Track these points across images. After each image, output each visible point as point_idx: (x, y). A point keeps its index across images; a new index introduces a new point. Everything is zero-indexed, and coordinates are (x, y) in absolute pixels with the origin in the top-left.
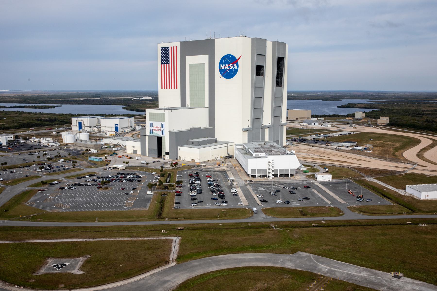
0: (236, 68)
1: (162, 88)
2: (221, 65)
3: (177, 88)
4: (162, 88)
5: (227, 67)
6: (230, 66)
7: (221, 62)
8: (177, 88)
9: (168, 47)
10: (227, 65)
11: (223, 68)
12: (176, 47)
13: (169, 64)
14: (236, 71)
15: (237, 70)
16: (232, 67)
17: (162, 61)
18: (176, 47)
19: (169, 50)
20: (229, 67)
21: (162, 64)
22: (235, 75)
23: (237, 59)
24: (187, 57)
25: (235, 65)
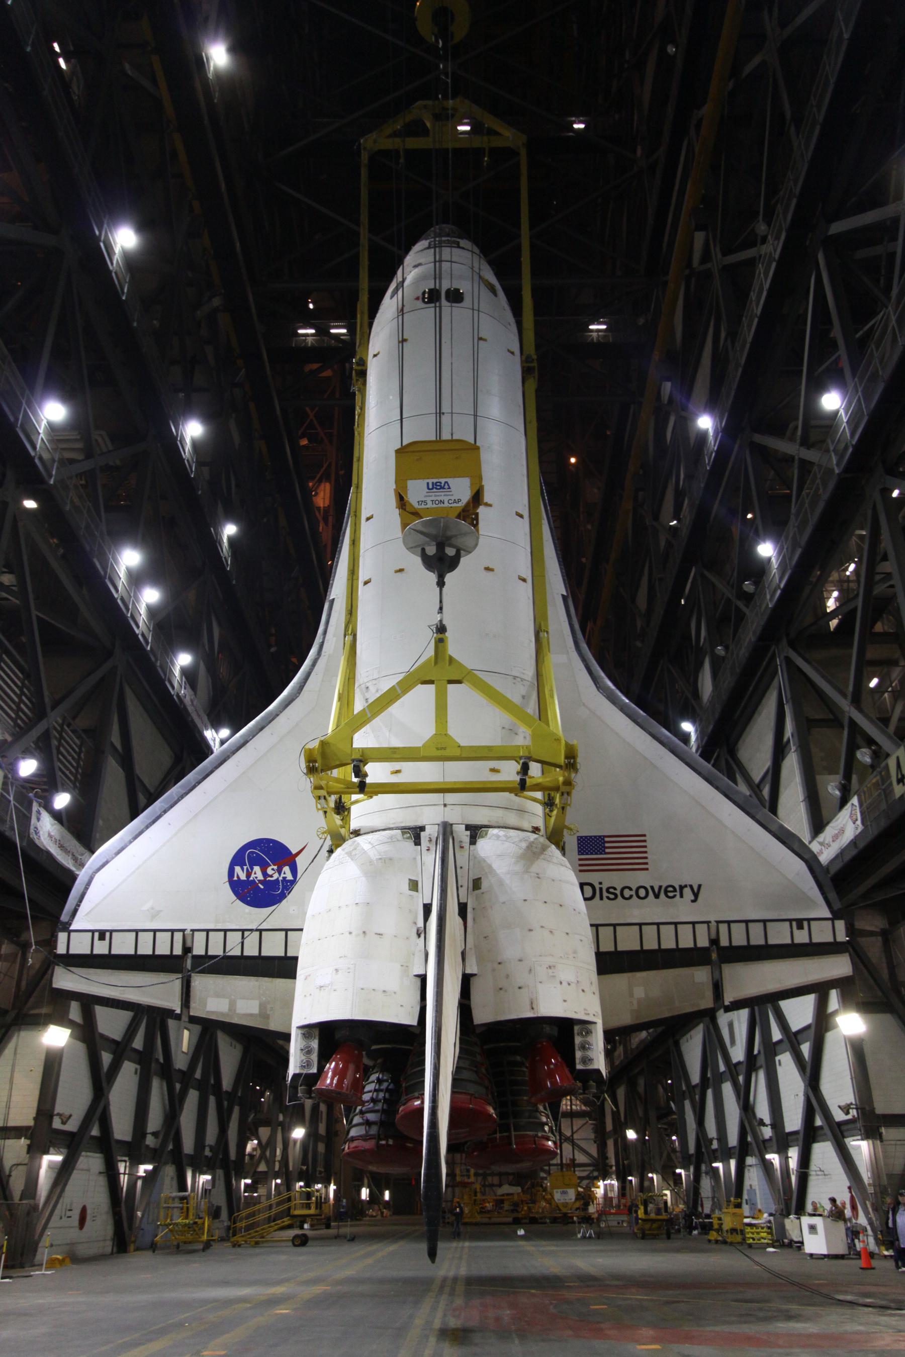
0: (289, 877)
2: (238, 869)
6: (269, 871)
7: (238, 859)
10: (257, 869)
11: (243, 877)
14: (288, 885)
15: (293, 882)
16: (276, 876)
20: (265, 874)
22: (282, 897)
23: (294, 852)
25: (286, 869)
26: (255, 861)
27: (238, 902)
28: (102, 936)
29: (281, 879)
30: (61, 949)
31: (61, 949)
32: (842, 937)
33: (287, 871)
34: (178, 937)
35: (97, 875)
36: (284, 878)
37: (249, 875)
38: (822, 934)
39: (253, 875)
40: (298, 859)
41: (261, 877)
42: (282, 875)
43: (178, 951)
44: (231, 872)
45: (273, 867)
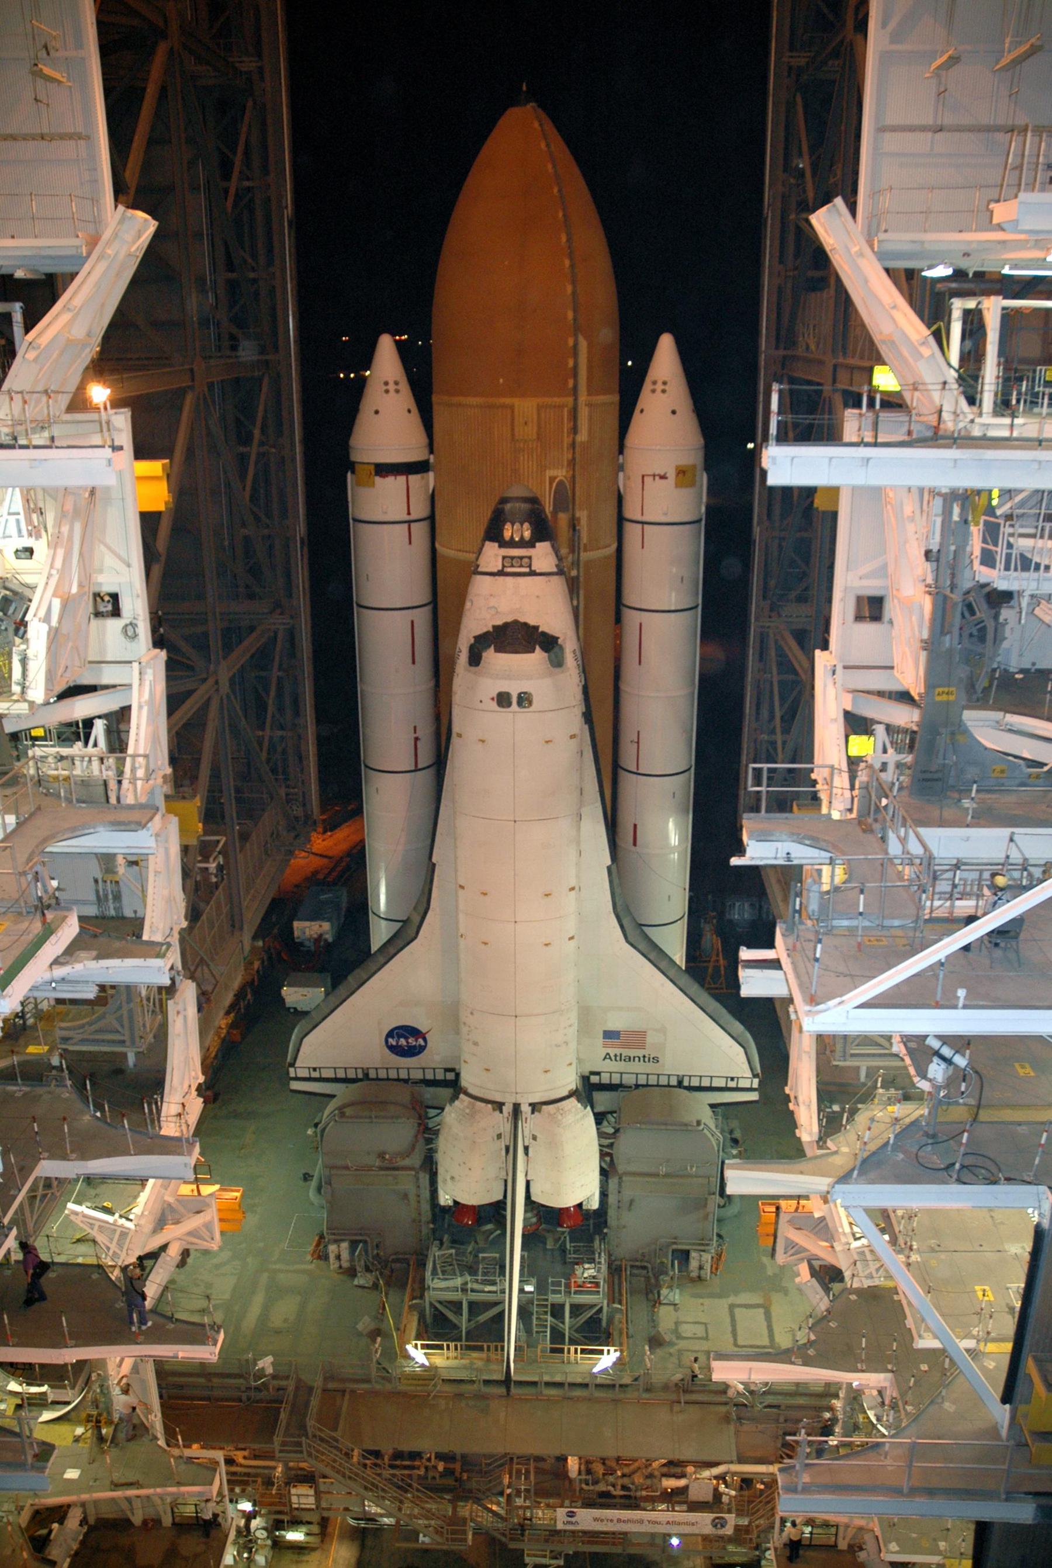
0: (423, 1043)
5: (403, 1042)
6: (410, 1041)
7: (390, 1034)
11: (394, 1043)
14: (422, 1049)
15: (425, 1047)
22: (419, 1053)
26: (399, 1036)
27: (394, 1056)
28: (315, 1069)
30: (292, 1075)
31: (292, 1075)
32: (756, 1084)
33: (421, 1042)
34: (360, 1071)
35: (305, 1040)
38: (744, 1084)
43: (360, 1076)
44: (387, 1041)
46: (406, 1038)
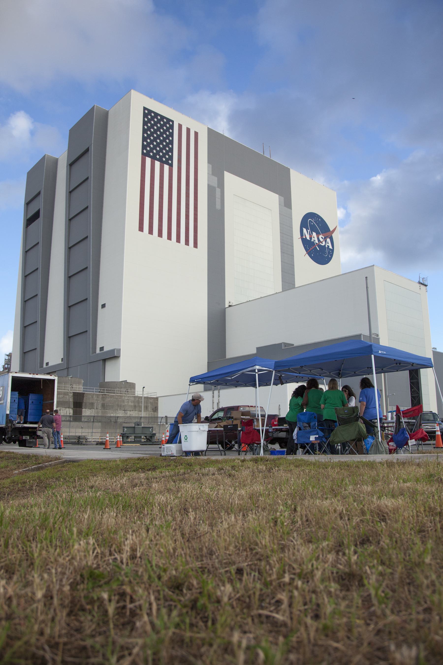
0: (331, 247)
1: (141, 229)
2: (305, 230)
3: (196, 245)
4: (141, 229)
7: (304, 224)
8: (196, 245)
9: (169, 120)
10: (314, 234)
11: (308, 238)
12: (196, 134)
13: (171, 165)
15: (333, 250)
17: (144, 147)
18: (196, 134)
19: (172, 127)
21: (143, 153)
23: (331, 229)
24: (226, 173)
25: (328, 240)
26: (313, 229)
29: (326, 246)
36: (328, 246)
37: (311, 238)
39: (313, 239)
40: (333, 235)
41: (317, 241)
42: (327, 244)
45: (322, 236)
46: (318, 234)
